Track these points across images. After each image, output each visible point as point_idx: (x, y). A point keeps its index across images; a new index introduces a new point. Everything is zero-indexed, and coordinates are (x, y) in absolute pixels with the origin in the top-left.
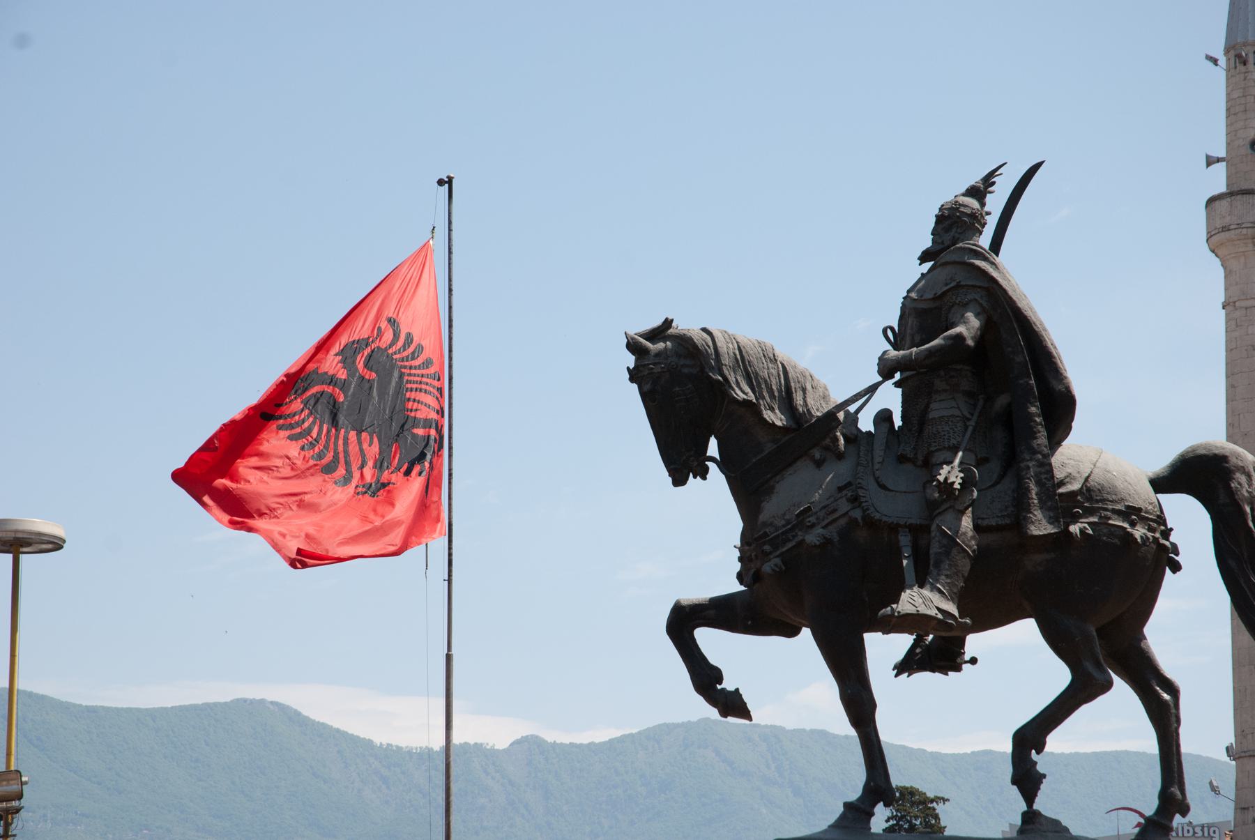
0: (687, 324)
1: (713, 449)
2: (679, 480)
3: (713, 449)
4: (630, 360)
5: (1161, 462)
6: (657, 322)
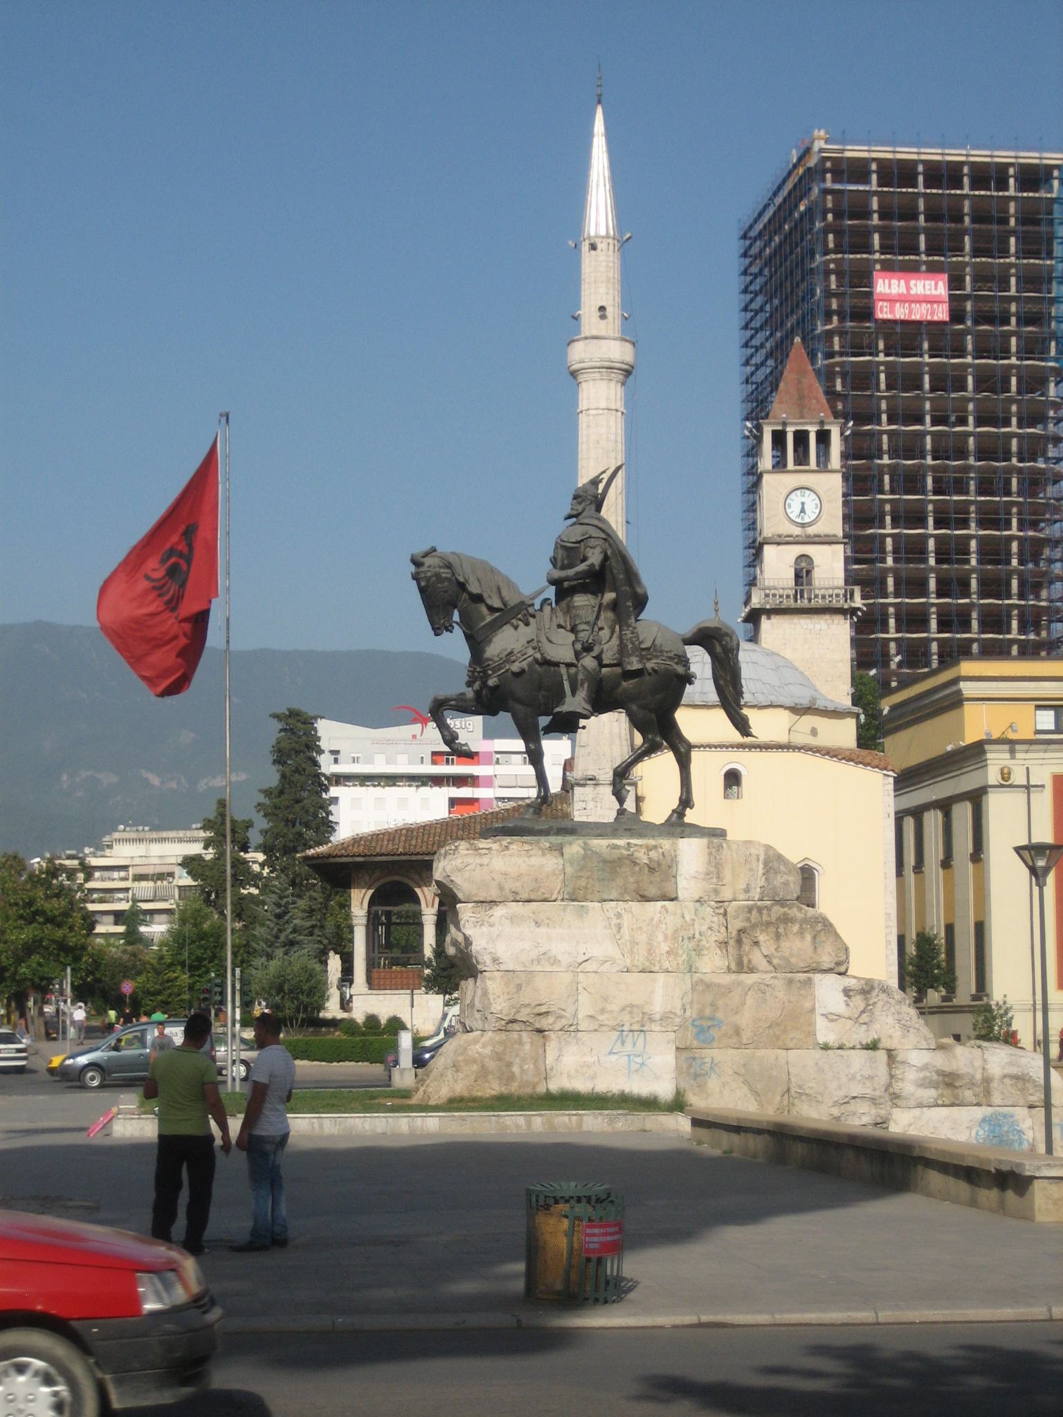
0: (444, 548)
1: (456, 616)
2: (437, 631)
3: (456, 616)
4: (412, 568)
5: (687, 629)
6: (425, 547)
